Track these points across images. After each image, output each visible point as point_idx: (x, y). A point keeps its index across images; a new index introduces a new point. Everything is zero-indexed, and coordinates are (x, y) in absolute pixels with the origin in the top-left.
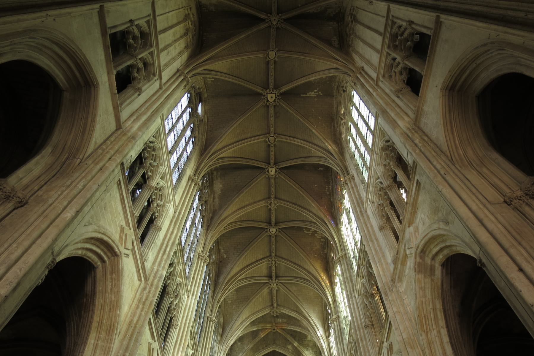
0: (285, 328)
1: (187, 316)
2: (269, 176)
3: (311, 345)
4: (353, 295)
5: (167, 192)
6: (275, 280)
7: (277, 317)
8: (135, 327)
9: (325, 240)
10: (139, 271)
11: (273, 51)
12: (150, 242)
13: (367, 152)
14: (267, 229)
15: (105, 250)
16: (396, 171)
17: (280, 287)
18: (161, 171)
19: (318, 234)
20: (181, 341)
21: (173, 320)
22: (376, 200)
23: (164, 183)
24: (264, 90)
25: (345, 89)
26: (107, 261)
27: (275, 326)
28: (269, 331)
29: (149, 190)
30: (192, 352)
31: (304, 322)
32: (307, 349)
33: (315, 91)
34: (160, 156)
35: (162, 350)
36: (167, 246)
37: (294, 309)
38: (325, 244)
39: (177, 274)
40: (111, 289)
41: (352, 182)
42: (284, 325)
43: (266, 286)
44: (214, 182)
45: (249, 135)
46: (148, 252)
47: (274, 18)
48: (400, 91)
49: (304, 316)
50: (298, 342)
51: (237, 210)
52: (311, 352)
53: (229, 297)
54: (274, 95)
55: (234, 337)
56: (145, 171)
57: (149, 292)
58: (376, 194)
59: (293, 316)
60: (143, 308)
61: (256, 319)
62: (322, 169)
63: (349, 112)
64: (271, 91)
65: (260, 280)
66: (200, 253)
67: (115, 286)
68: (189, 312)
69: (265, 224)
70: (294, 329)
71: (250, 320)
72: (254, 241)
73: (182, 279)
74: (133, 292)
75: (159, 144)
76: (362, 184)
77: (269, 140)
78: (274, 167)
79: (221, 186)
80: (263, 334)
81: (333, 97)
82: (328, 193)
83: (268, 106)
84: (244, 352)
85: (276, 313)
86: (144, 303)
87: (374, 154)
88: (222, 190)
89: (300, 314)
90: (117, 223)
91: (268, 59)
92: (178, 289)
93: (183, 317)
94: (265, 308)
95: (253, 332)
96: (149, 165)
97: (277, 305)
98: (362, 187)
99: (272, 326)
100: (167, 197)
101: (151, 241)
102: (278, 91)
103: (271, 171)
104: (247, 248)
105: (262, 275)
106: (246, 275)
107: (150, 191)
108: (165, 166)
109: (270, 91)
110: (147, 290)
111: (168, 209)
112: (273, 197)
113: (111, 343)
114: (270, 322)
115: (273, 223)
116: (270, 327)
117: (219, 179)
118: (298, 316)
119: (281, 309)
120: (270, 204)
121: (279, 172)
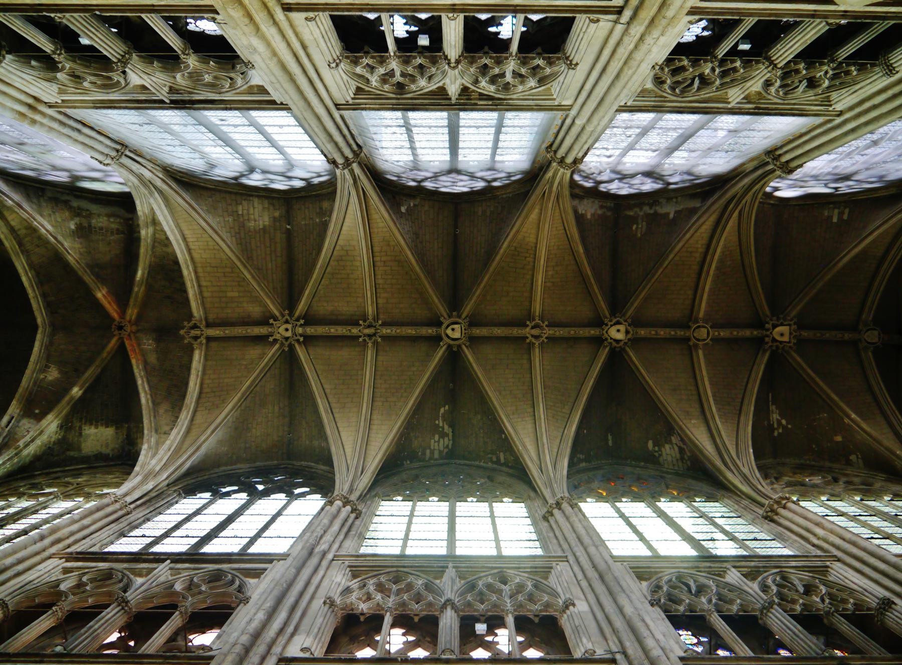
2: (607, 325)
9: (427, 459)
11: (879, 338)
14: (459, 316)
17: (277, 346)
19: (439, 442)
28: (115, 315)
33: (784, 422)
37: (205, 386)
38: (420, 461)
44: (596, 202)
52: (53, 440)
53: (251, 211)
62: (610, 443)
77: (699, 327)
79: (589, 217)
80: (104, 295)
84: (55, 238)
88: (582, 215)
97: (209, 339)
99: (130, 322)
116: (128, 318)
117: (600, 212)
118: (192, 398)
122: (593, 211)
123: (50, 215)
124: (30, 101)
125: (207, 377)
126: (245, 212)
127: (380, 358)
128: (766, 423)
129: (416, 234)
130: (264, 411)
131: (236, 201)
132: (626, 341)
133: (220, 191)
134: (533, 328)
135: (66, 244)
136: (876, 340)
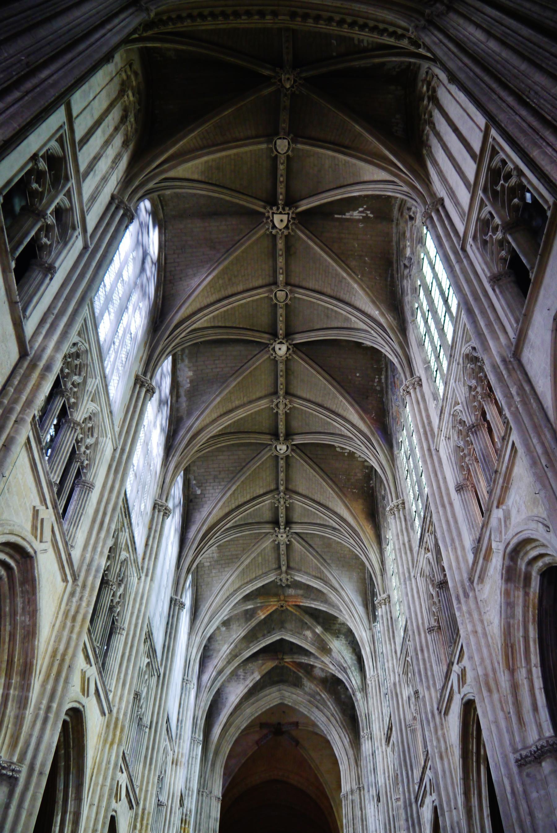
0: (301, 604)
1: (139, 611)
2: (275, 357)
3: (344, 630)
4: (412, 575)
5: (101, 420)
6: (285, 529)
7: (288, 586)
8: (63, 660)
10: (63, 567)
11: (284, 138)
12: (78, 513)
13: (444, 351)
14: (270, 445)
15: (12, 552)
16: (485, 407)
17: (292, 539)
18: (90, 390)
20: (130, 655)
21: (117, 620)
22: (455, 436)
23: (96, 405)
24: (268, 208)
25: (413, 215)
26: (15, 568)
27: (283, 601)
28: (274, 608)
29: (72, 430)
30: (147, 660)
31: (333, 597)
32: (338, 637)
33: (361, 209)
34: (87, 364)
35: (102, 676)
36: (105, 514)
37: (317, 575)
39: (121, 548)
40: (23, 608)
41: (418, 390)
42: (299, 600)
43: (269, 539)
45: (240, 288)
46: (75, 533)
47: (287, 76)
48: (498, 280)
49: (331, 585)
50: (322, 627)
51: (218, 417)
52: (345, 642)
54: (285, 217)
55: (214, 623)
56: (64, 401)
57: (81, 599)
58: (454, 427)
59: (315, 586)
60: (73, 627)
61: (252, 592)
63: (419, 262)
64: (281, 210)
65: (259, 529)
66: (156, 500)
67: (29, 602)
68: (141, 604)
69: (269, 437)
70: (317, 607)
71: (242, 593)
72: (248, 466)
73: (129, 552)
74: (56, 602)
75: (85, 344)
76: (434, 400)
78: (284, 341)
80: (263, 614)
81: (393, 221)
82: (378, 388)
83: (274, 237)
85: (286, 581)
86: (74, 619)
87: (453, 362)
88: (191, 382)
89: (326, 582)
90: (28, 505)
91: (275, 153)
92: (123, 570)
93: (132, 613)
94: (266, 574)
95: (246, 611)
96: (71, 386)
97: (289, 567)
98: (434, 406)
99: (278, 601)
100: (100, 428)
101: (79, 511)
102: (293, 209)
103: (280, 349)
104: (236, 478)
105: (262, 521)
106: (236, 522)
107: (75, 432)
108: (96, 378)
109: (278, 209)
110: (77, 595)
111: (103, 447)
112: (281, 392)
113: (28, 690)
114: (276, 595)
115: (281, 435)
117: (186, 361)
118: (323, 587)
119: (295, 575)
120: (277, 405)
121: (293, 351)
122: (187, 369)
123: (219, 644)
124: (174, 766)
125: (311, 573)
126: (208, 560)
127: (300, 491)
128: (361, 225)
129: (215, 477)
130: (333, 545)
131: (202, 567)
132: (288, 344)
133: (197, 579)
134: (278, 408)
135: (234, 637)
136: (286, 142)
